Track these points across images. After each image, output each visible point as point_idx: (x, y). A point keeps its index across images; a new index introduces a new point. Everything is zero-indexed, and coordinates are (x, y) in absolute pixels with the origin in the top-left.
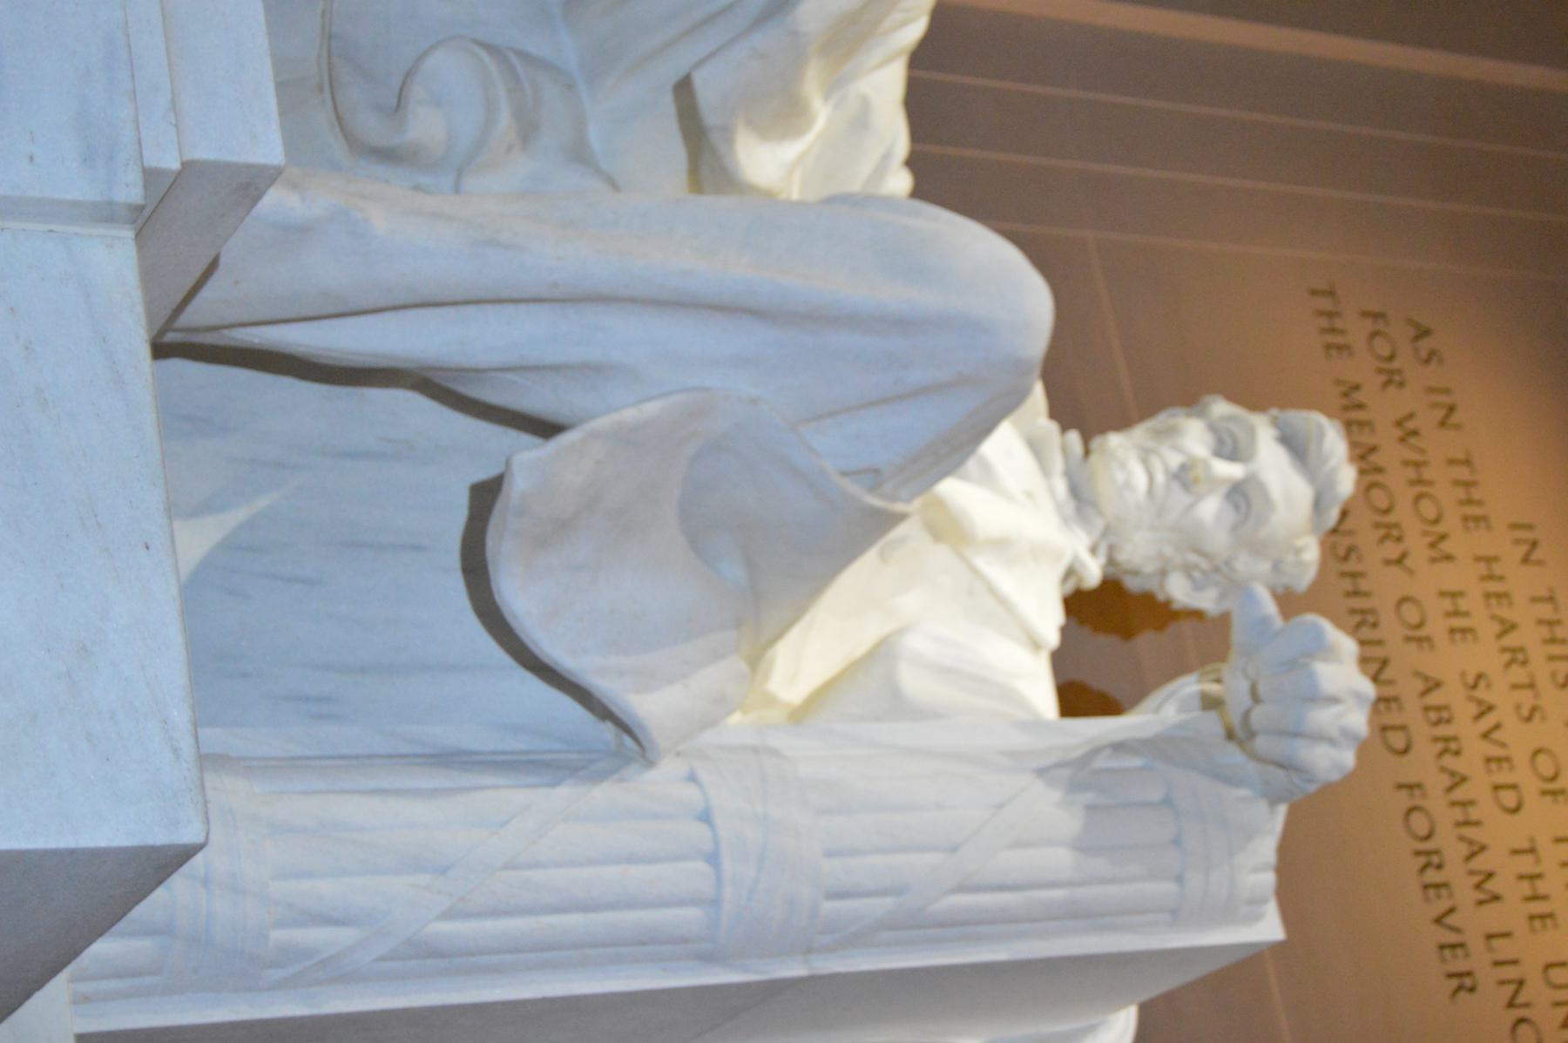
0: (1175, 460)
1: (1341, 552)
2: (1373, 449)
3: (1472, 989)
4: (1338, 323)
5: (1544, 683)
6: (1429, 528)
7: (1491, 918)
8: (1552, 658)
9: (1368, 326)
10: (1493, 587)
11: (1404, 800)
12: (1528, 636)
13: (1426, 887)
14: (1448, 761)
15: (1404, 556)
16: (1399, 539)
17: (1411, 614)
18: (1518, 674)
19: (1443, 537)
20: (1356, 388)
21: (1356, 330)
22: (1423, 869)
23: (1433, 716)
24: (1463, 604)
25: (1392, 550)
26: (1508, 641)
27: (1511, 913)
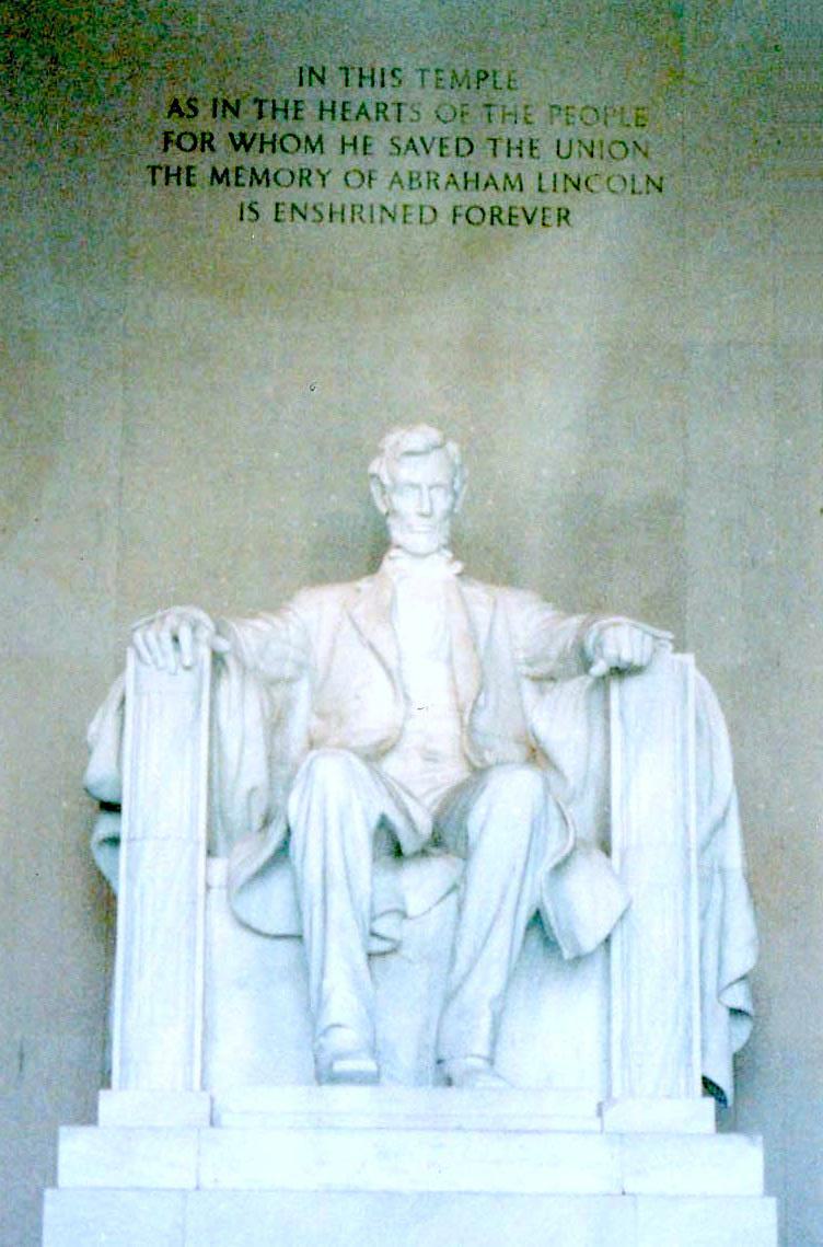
0: (414, 519)
1: (318, 217)
2: (253, 171)
3: (568, 212)
4: (173, 170)
5: (400, 96)
6: (303, 144)
7: (530, 183)
8: (383, 85)
9: (173, 148)
10: (339, 109)
11: (461, 220)
12: (368, 95)
13: (510, 223)
14: (442, 181)
15: (319, 171)
16: (310, 174)
17: (354, 179)
18: (391, 112)
19: (308, 139)
20: (214, 171)
21: (177, 158)
22: (500, 221)
23: (415, 184)
24: (349, 140)
25: (315, 179)
26: (372, 113)
27: (529, 169)
